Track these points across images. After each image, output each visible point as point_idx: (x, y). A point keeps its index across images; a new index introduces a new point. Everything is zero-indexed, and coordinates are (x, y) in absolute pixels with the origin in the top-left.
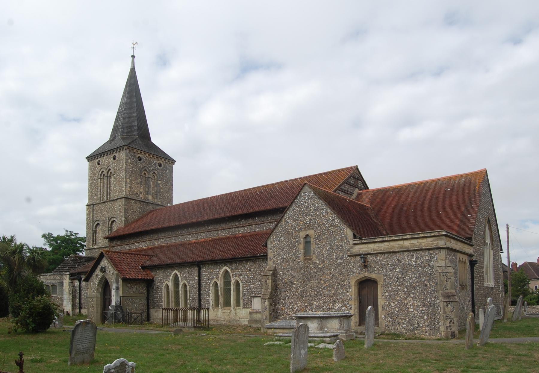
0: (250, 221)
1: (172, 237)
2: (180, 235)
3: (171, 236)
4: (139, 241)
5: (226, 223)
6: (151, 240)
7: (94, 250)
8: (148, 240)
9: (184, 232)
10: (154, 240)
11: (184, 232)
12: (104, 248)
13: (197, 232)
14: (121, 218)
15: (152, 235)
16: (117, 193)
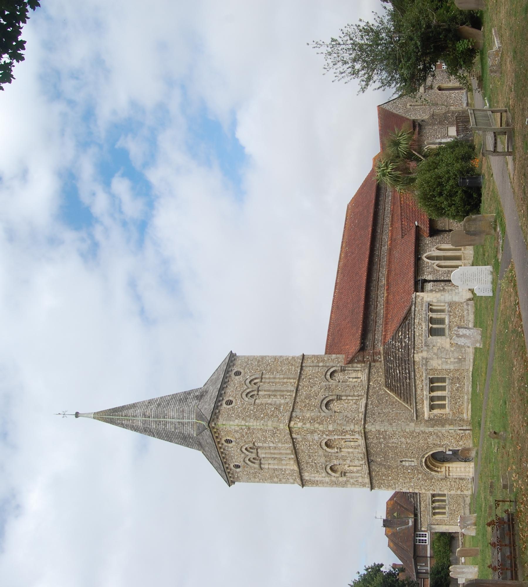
0: (381, 203)
1: (380, 264)
2: (379, 256)
3: (379, 265)
4: (375, 304)
5: (378, 219)
6: (378, 289)
7: (370, 407)
8: (376, 292)
9: (377, 253)
10: (378, 284)
11: (377, 253)
12: (368, 388)
13: (381, 241)
14: (332, 359)
15: (372, 288)
16: (292, 368)
